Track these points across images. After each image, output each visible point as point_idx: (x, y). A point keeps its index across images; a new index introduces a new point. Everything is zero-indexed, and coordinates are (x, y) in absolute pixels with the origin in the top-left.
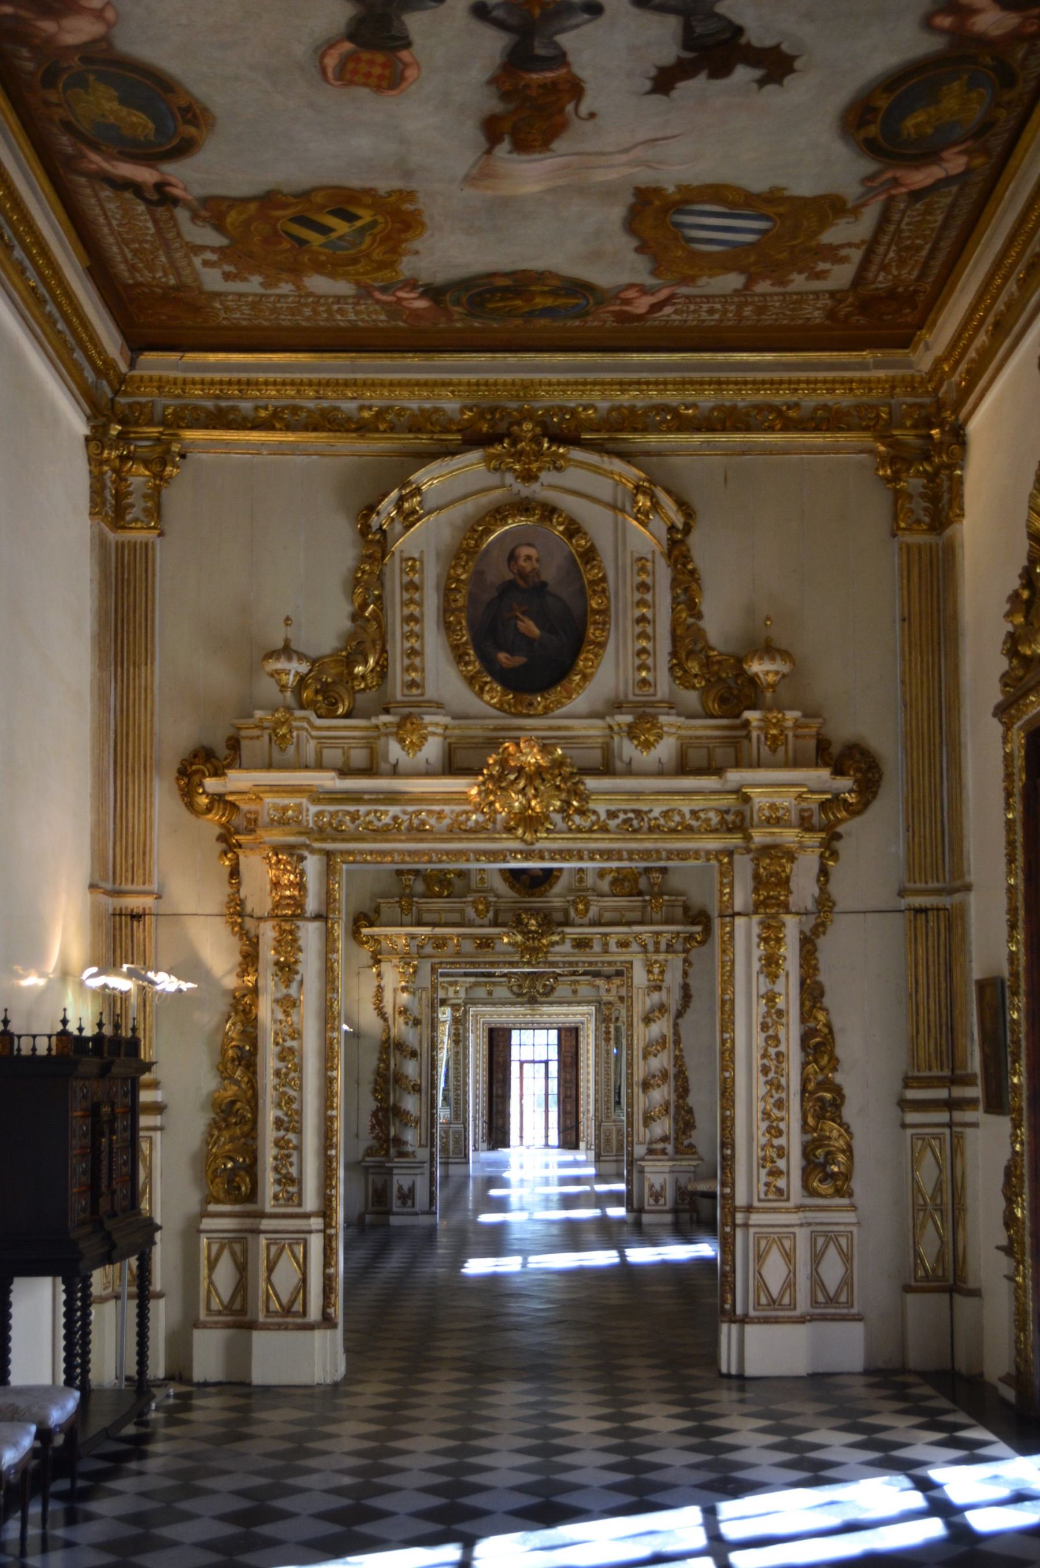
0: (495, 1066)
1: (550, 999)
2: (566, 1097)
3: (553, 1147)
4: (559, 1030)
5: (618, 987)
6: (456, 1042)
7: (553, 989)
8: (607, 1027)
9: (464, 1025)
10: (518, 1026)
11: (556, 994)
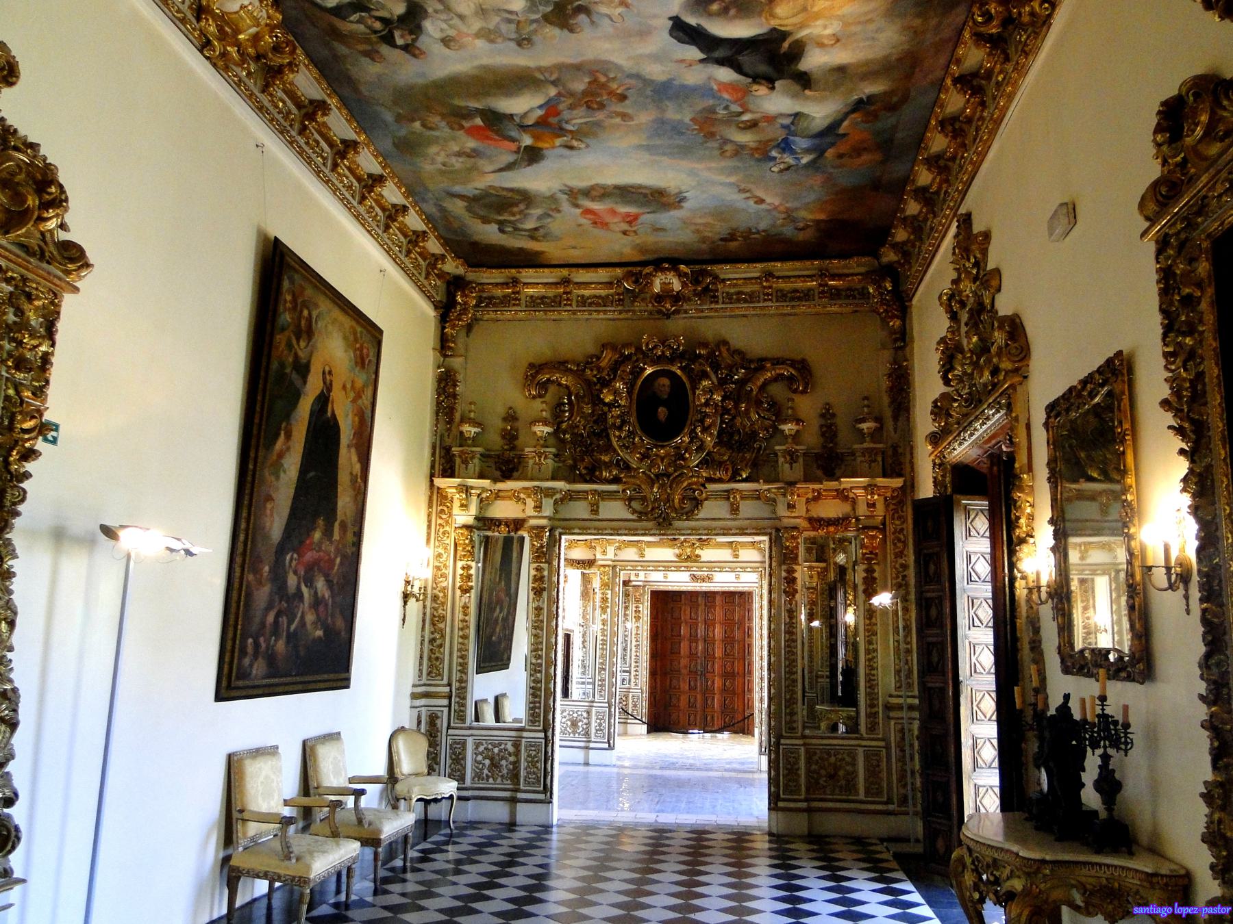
5: (808, 501)
6: (538, 592)
8: (791, 571)
9: (549, 562)
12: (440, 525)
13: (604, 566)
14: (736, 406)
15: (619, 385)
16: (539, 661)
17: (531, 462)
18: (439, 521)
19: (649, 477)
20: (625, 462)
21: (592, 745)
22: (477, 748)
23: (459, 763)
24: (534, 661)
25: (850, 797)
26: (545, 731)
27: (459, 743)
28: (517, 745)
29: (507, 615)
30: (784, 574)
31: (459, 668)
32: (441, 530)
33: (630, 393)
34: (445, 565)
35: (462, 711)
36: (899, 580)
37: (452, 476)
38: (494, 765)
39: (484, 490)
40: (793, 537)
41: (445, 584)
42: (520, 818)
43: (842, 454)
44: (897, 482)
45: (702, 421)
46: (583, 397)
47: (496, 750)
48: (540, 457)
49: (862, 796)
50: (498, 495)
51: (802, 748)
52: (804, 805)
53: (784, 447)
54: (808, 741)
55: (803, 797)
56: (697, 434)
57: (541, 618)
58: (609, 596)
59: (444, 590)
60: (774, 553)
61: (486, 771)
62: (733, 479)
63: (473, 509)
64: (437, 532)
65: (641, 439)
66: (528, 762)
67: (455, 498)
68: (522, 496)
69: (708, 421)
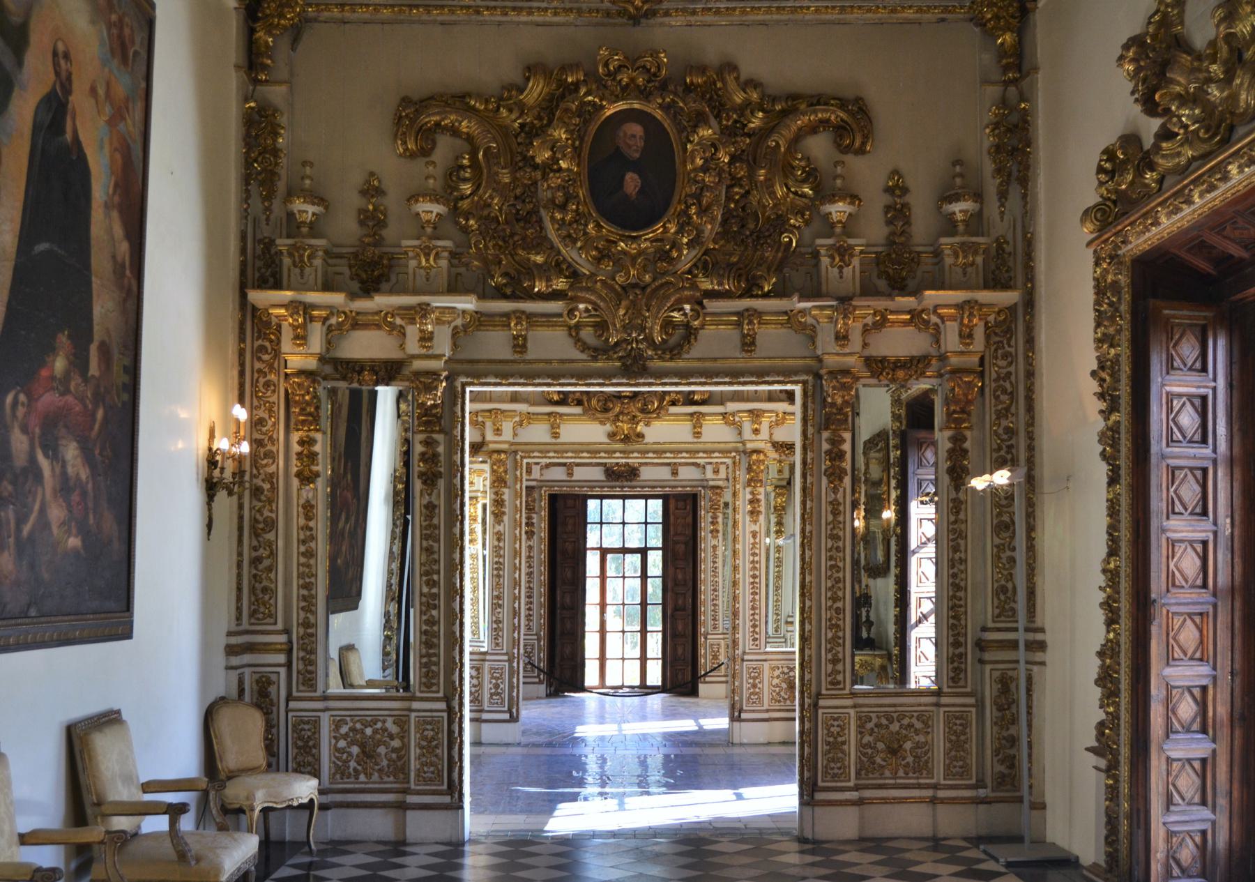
0: (559, 558)
1: (680, 364)
2: (675, 609)
3: (654, 690)
4: (666, 499)
5: (866, 330)
7: (690, 334)
8: (836, 442)
9: (447, 432)
10: (597, 491)
11: (699, 349)
12: (259, 371)
13: (499, 452)
14: (751, 175)
15: (561, 134)
16: (435, 590)
17: (413, 263)
18: (258, 365)
19: (611, 288)
20: (570, 266)
21: (485, 716)
22: (338, 727)
23: (309, 753)
24: (425, 590)
25: (922, 781)
26: (448, 699)
27: (308, 722)
28: (402, 722)
29: (355, 528)
30: (826, 446)
31: (303, 604)
32: (262, 380)
33: (577, 151)
34: (271, 438)
35: (310, 672)
36: (1003, 453)
37: (278, 286)
38: (368, 754)
39: (332, 310)
40: (844, 387)
41: (272, 469)
42: (412, 833)
43: (919, 253)
44: (1009, 297)
45: (698, 197)
46: (497, 156)
47: (369, 731)
48: (427, 255)
49: (939, 776)
50: (357, 322)
51: (852, 712)
52: (854, 795)
53: (830, 241)
54: (861, 701)
55: (851, 784)
56: (690, 217)
57: (435, 521)
58: (506, 497)
59: (271, 478)
60: (810, 412)
61: (353, 764)
62: (747, 293)
63: (316, 342)
64: (254, 384)
65: (598, 226)
66: (422, 748)
67: (285, 324)
68: (398, 321)
69: (707, 197)
